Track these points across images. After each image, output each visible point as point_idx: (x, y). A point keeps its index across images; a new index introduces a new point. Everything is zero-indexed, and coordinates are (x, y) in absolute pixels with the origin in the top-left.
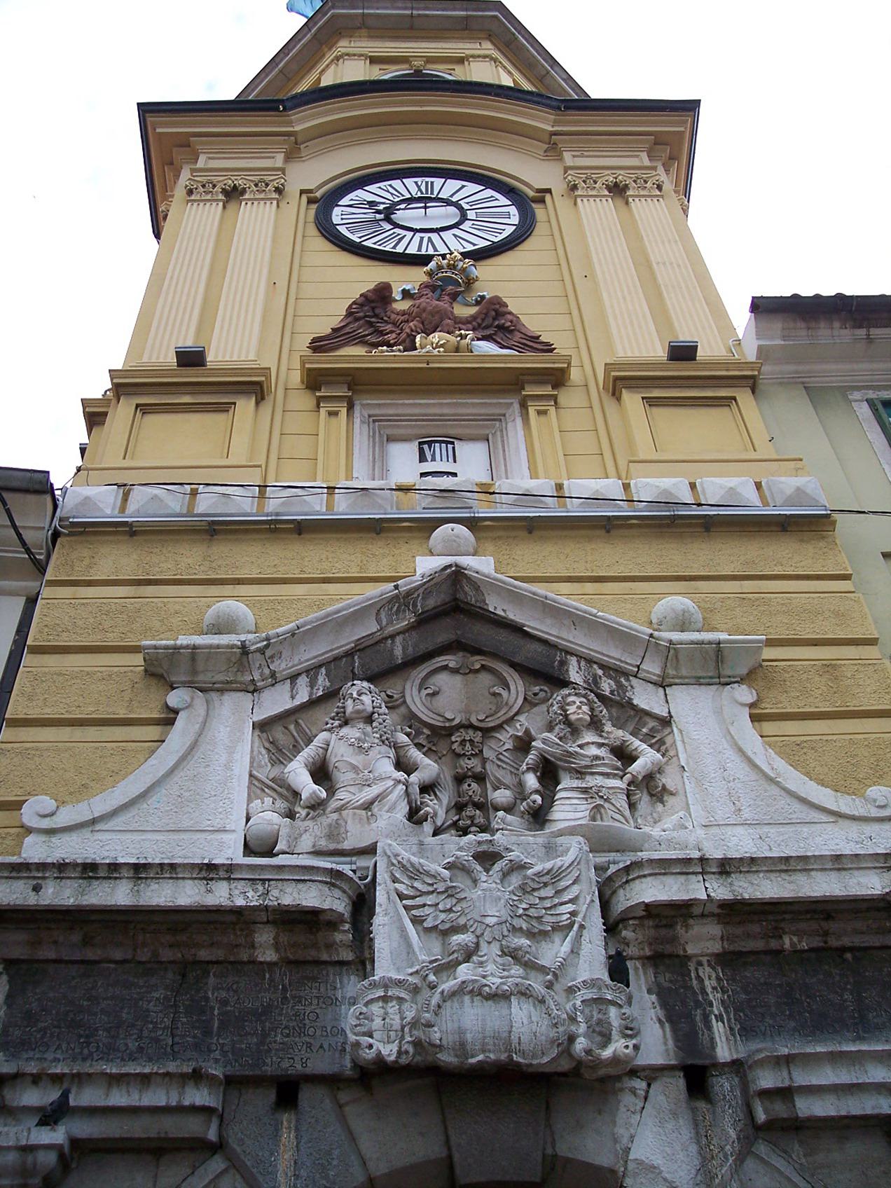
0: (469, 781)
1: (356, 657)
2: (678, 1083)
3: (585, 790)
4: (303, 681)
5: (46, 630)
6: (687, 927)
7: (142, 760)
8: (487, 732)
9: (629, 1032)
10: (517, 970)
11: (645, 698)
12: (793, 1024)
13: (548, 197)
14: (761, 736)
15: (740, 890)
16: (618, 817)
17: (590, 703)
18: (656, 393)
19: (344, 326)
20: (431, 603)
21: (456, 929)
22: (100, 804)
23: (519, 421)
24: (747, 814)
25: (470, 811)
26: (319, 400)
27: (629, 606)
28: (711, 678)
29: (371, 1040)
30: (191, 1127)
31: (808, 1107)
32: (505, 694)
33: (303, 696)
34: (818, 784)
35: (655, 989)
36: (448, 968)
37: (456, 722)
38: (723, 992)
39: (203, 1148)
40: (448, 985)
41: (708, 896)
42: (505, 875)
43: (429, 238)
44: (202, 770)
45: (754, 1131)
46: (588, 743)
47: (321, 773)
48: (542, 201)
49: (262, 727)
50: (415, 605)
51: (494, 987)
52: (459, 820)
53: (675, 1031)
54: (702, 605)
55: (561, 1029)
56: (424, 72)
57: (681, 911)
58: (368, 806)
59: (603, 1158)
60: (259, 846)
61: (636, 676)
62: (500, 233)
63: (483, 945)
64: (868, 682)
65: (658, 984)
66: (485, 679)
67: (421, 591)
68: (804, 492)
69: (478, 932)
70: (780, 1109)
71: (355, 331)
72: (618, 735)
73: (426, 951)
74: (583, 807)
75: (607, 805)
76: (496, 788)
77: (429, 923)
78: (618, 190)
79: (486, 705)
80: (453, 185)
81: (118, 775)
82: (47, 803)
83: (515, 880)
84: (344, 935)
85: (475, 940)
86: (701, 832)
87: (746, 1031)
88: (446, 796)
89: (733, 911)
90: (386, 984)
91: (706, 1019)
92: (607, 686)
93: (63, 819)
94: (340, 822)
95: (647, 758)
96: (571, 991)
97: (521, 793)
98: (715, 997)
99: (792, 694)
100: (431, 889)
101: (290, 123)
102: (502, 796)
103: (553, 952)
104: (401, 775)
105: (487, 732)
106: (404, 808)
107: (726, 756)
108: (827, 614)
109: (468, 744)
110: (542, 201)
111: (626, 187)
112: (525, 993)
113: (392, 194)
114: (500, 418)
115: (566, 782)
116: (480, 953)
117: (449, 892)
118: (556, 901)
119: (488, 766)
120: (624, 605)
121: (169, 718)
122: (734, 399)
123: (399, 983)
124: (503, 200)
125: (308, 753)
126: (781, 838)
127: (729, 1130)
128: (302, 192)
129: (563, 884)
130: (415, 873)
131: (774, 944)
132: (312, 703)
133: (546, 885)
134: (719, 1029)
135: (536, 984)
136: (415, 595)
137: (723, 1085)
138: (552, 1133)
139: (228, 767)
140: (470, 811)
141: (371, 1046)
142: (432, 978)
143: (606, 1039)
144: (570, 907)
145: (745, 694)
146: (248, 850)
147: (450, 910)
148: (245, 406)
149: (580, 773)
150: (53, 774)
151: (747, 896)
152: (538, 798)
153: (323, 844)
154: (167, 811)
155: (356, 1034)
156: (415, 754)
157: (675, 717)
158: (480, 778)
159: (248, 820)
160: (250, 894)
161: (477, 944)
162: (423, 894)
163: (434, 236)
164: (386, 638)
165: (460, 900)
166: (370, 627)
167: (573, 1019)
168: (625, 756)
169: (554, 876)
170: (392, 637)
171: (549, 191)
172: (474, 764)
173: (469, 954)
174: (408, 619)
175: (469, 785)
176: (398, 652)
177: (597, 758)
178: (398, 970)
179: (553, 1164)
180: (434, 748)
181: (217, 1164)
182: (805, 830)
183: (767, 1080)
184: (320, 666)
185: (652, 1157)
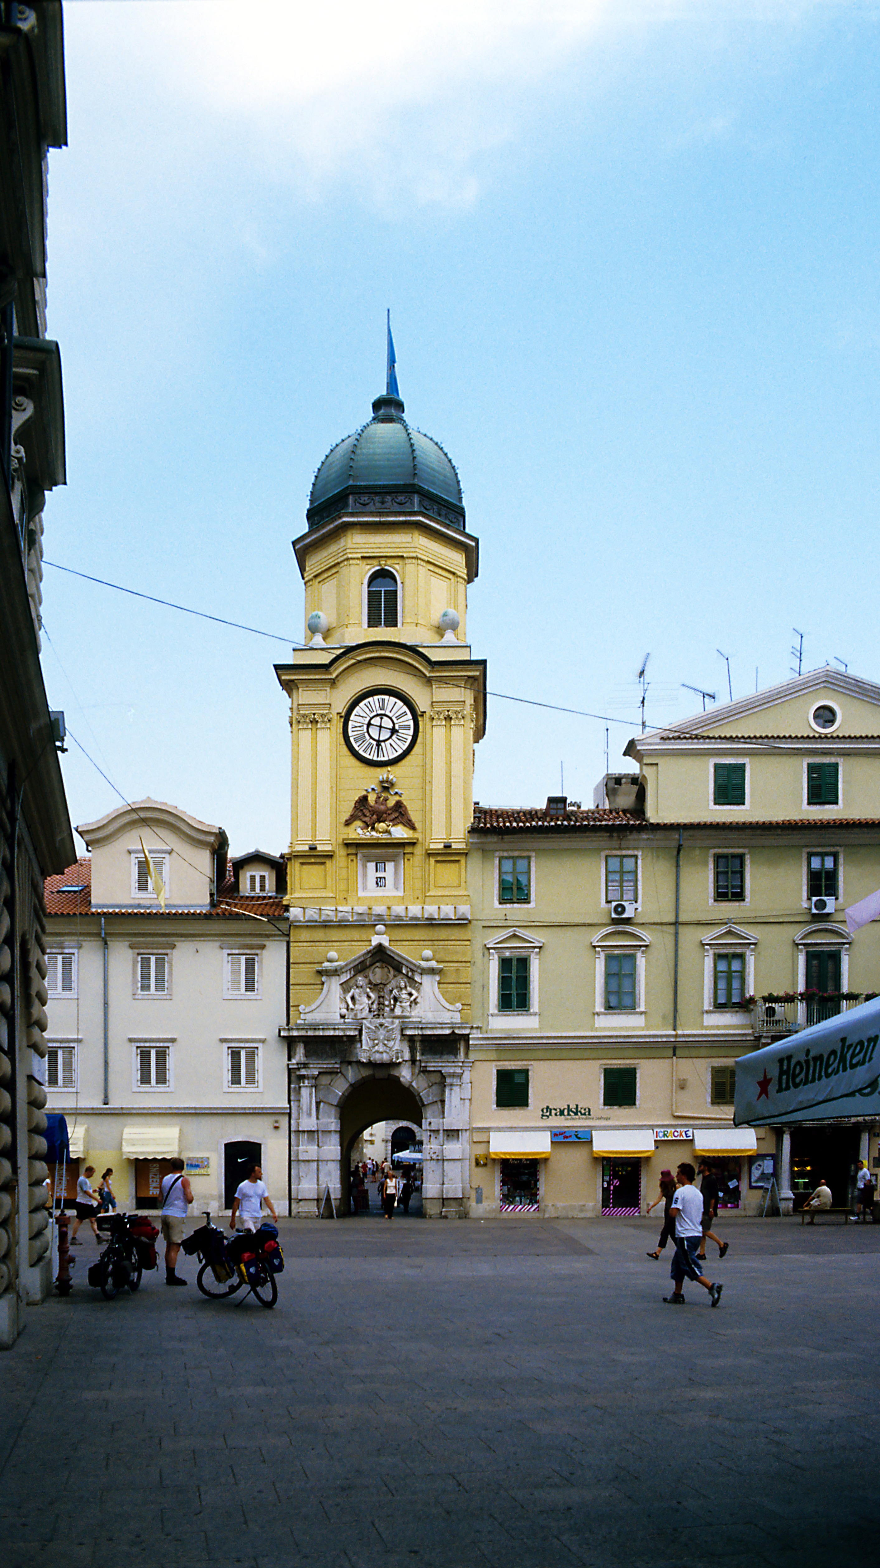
2: (410, 1063)
4: (348, 972)
8: (385, 985)
11: (417, 978)
18: (439, 859)
21: (375, 1039)
22: (313, 1007)
26: (348, 855)
30: (335, 1070)
31: (429, 1069)
33: (349, 977)
36: (374, 1047)
39: (337, 1073)
40: (373, 1051)
45: (420, 1072)
47: (353, 998)
48: (422, 716)
49: (341, 984)
59: (397, 1075)
66: (386, 969)
70: (424, 1069)
73: (370, 1043)
78: (448, 718)
79: (386, 977)
80: (393, 700)
81: (316, 999)
87: (422, 1054)
88: (376, 1003)
92: (410, 974)
93: (307, 1011)
97: (390, 1004)
98: (418, 1048)
101: (331, 674)
102: (387, 1003)
103: (391, 1044)
105: (385, 985)
106: (368, 1009)
110: (422, 716)
112: (386, 1052)
115: (398, 1003)
117: (375, 1032)
121: (323, 984)
124: (409, 716)
125: (350, 994)
127: (417, 1071)
130: (369, 1028)
132: (351, 978)
134: (418, 1054)
137: (418, 1063)
145: (437, 978)
148: (328, 863)
149: (401, 1002)
156: (371, 995)
166: (362, 959)
168: (410, 994)
169: (392, 1029)
171: (425, 712)
172: (382, 994)
173: (377, 1044)
174: (370, 955)
176: (368, 963)
179: (390, 1075)
181: (340, 1075)
183: (423, 1064)
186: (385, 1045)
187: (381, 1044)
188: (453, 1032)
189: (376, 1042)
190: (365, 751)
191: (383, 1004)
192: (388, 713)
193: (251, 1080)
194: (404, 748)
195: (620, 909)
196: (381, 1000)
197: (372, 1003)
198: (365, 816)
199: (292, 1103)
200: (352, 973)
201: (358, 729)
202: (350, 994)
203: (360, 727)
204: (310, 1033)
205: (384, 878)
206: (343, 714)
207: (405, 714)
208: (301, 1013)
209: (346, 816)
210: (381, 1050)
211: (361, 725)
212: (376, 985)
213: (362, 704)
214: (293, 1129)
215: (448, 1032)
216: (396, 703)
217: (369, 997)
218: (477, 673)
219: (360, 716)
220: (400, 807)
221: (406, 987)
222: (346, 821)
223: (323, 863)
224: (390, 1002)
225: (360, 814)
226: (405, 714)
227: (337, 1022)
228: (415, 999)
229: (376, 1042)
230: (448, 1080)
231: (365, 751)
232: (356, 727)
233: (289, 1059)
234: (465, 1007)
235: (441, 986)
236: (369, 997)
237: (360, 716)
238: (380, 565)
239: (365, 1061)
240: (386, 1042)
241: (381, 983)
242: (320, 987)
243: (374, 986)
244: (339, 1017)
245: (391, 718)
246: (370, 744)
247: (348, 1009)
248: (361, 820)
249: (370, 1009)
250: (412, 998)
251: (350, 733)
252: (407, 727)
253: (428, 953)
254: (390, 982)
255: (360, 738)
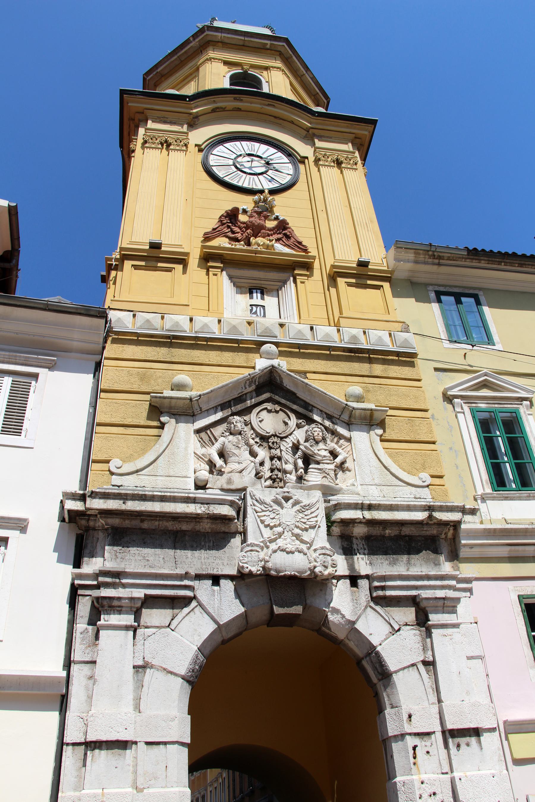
0: (276, 459)
1: (232, 402)
3: (319, 469)
5: (108, 381)
6: (353, 527)
7: (153, 445)
9: (334, 566)
10: (298, 542)
12: (387, 562)
13: (306, 160)
14: (384, 448)
15: (374, 516)
16: (331, 481)
17: (322, 431)
19: (218, 227)
20: (262, 380)
22: (140, 464)
23: (293, 285)
24: (377, 481)
25: (276, 472)
27: (337, 387)
28: (367, 422)
29: (248, 566)
32: (289, 422)
34: (402, 470)
35: (341, 547)
37: (270, 434)
38: (365, 549)
40: (273, 546)
41: (363, 517)
42: (294, 505)
43: (253, 178)
44: (176, 450)
46: (321, 449)
47: (222, 454)
50: (255, 382)
51: (290, 548)
52: (272, 475)
53: (347, 563)
54: (365, 389)
55: (312, 564)
56: (249, 72)
57: (352, 522)
58: (241, 472)
60: (201, 486)
61: (338, 419)
62: (285, 179)
63: (286, 532)
64: (424, 428)
65: (343, 546)
66: (282, 415)
67: (258, 375)
68: (408, 341)
69: (284, 528)
71: (222, 230)
72: (332, 445)
74: (319, 477)
75: (328, 476)
76: (286, 463)
77: (266, 523)
81: (144, 451)
82: (118, 462)
83: (297, 507)
85: (283, 530)
86: (360, 487)
88: (268, 465)
89: (371, 523)
90: (252, 545)
91: (358, 558)
94: (231, 477)
96: (315, 550)
99: (396, 431)
100: (267, 509)
104: (252, 459)
105: (282, 438)
106: (254, 472)
107: (370, 456)
108: (412, 397)
109: (275, 443)
111: (342, 163)
113: (236, 150)
114: (285, 282)
116: (284, 535)
118: (310, 516)
119: (283, 452)
120: (335, 386)
121: (162, 426)
122: (382, 286)
123: (257, 545)
125: (217, 445)
126: (388, 491)
128: (196, 145)
129: (313, 510)
130: (262, 503)
131: (382, 533)
133: (307, 510)
135: (304, 547)
136: (255, 378)
138: (305, 597)
139: (186, 449)
140: (276, 472)
141: (247, 568)
142: (268, 544)
143: (326, 567)
144: (315, 519)
146: (198, 487)
147: (274, 518)
149: (318, 463)
150: (118, 448)
151: (376, 518)
152: (302, 470)
153: (225, 486)
154: (164, 467)
155: (242, 563)
157: (352, 439)
158: (280, 459)
159: (195, 473)
160: (203, 508)
161: (284, 532)
162: (263, 511)
163: (255, 177)
164: (243, 395)
165: (278, 514)
167: (316, 561)
169: (309, 506)
170: (246, 394)
171: (307, 158)
173: (280, 535)
174: (253, 387)
175: (276, 461)
177: (325, 456)
178: (256, 539)
180: (262, 444)
181: (194, 604)
182: (397, 488)
184: (219, 405)
185: (338, 607)
186: (297, 536)
187: (287, 534)
188: (430, 517)
189: (279, 529)
197: (262, 464)
198: (233, 232)
199: (74, 668)
204: (132, 506)
205: (263, 307)
206: (203, 147)
208: (112, 474)
210: (290, 548)
212: (264, 439)
215: (421, 516)
216: (268, 149)
217: (253, 454)
218: (366, 133)
219: (224, 152)
220: (285, 228)
222: (205, 234)
223: (169, 270)
225: (226, 230)
227: (191, 491)
228: (343, 463)
229: (279, 529)
230: (434, 618)
234: (437, 481)
235: (387, 444)
236: (253, 454)
237: (224, 152)
238: (242, 69)
239: (254, 569)
240: (297, 531)
241: (275, 436)
242: (155, 432)
244: (192, 486)
248: (227, 237)
249: (257, 474)
250: (338, 460)
253: (357, 389)
254: (291, 434)
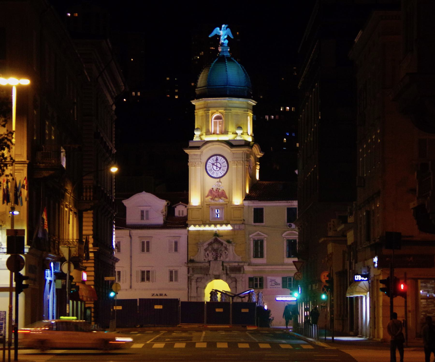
8: (218, 249)
11: (228, 247)
18: (235, 209)
47: (208, 254)
66: (218, 245)
84: (209, 266)
88: (215, 255)
95: (227, 253)
102: (218, 255)
115: (222, 256)
156: (213, 253)
168: (226, 253)
172: (217, 252)
190: (212, 174)
191: (217, 255)
192: (219, 162)
193: (176, 280)
194: (224, 172)
195: (290, 226)
196: (217, 254)
197: (214, 255)
200: (208, 246)
201: (210, 167)
202: (207, 253)
203: (210, 166)
207: (224, 162)
209: (206, 195)
211: (211, 165)
213: (211, 159)
214: (189, 296)
221: (224, 250)
224: (219, 255)
226: (224, 162)
231: (212, 174)
232: (209, 166)
233: (188, 273)
241: (217, 249)
243: (215, 250)
244: (203, 260)
245: (220, 163)
246: (214, 172)
247: (206, 257)
250: (227, 254)
251: (207, 168)
252: (225, 166)
255: (211, 170)
